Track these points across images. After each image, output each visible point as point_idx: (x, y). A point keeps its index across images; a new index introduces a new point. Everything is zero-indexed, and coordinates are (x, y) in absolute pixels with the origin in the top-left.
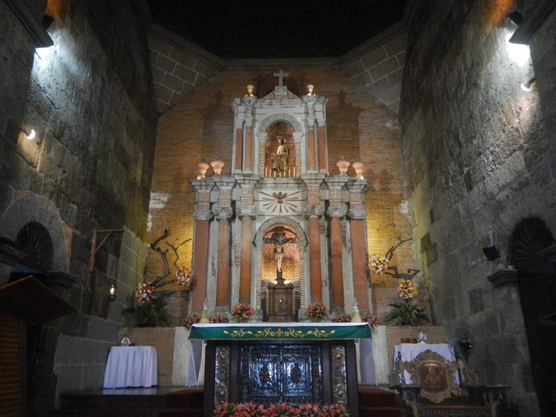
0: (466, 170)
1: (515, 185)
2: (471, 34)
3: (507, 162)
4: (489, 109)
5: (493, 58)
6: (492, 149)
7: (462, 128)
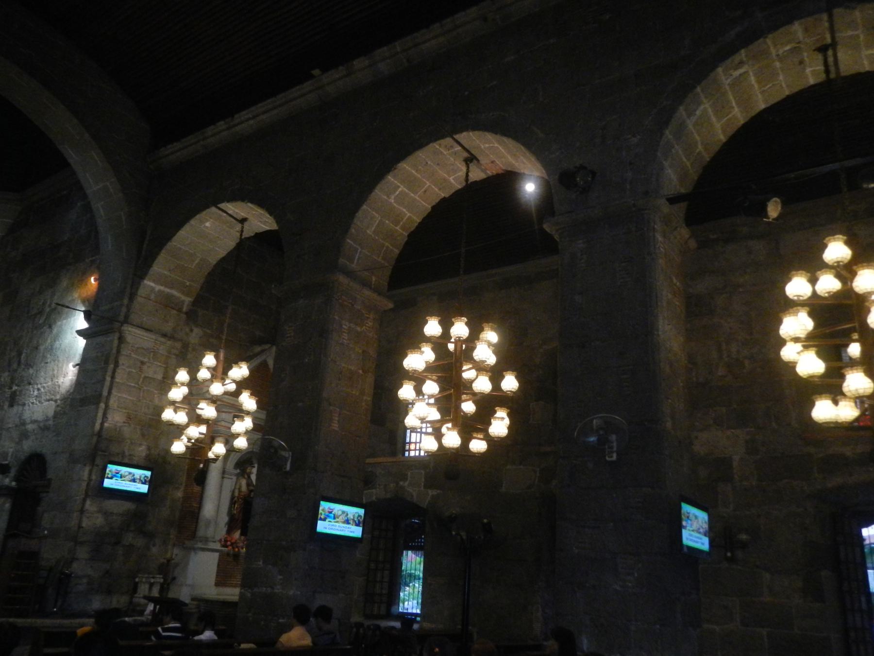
0: (15, 388)
1: (42, 425)
2: (65, 283)
3: (44, 404)
4: (50, 355)
5: (69, 319)
6: (39, 386)
7: (26, 350)
